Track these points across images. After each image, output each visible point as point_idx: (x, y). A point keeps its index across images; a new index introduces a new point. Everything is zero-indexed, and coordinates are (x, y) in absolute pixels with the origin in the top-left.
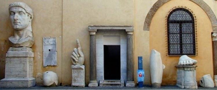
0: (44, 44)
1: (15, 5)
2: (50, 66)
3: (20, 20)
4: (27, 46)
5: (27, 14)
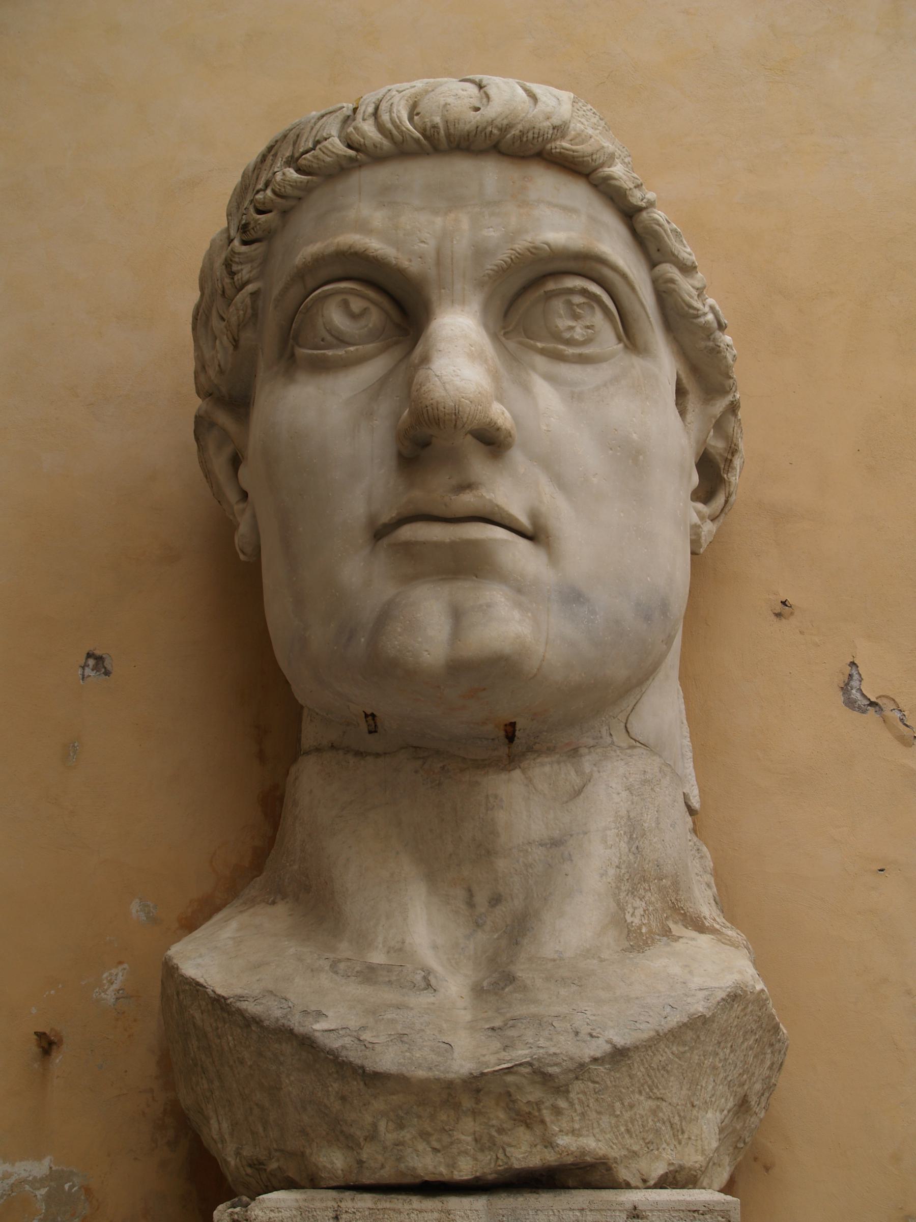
1: (413, 111)
4: (692, 1158)
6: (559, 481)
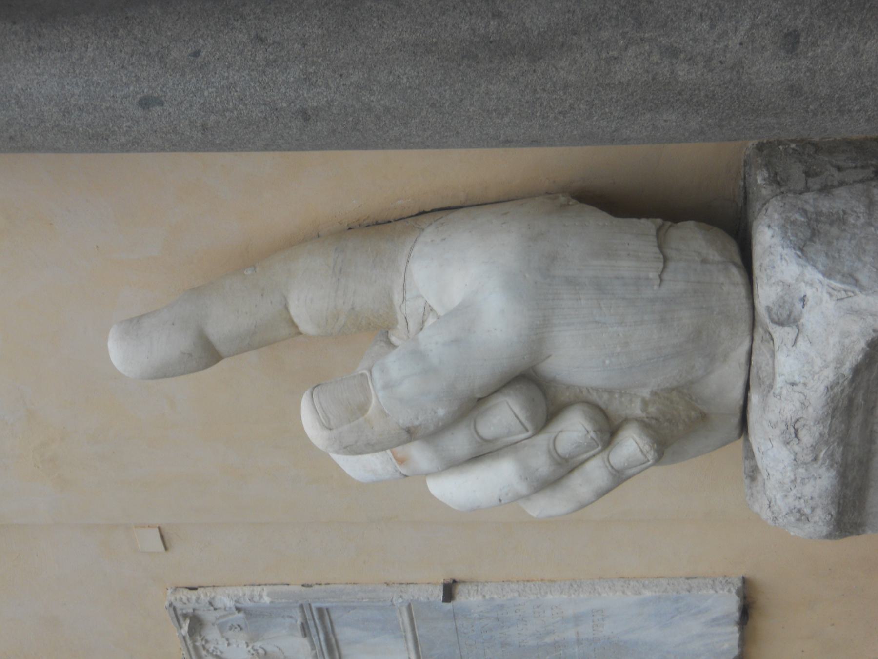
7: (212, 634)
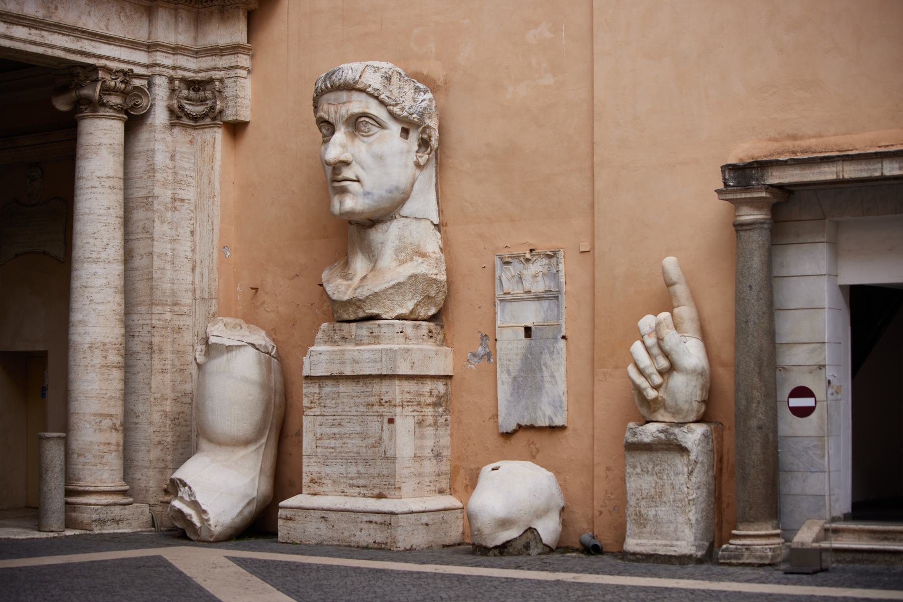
0: (499, 292)
2: (532, 428)
3: (360, 164)
5: (395, 129)
6: (363, 168)
7: (545, 261)
